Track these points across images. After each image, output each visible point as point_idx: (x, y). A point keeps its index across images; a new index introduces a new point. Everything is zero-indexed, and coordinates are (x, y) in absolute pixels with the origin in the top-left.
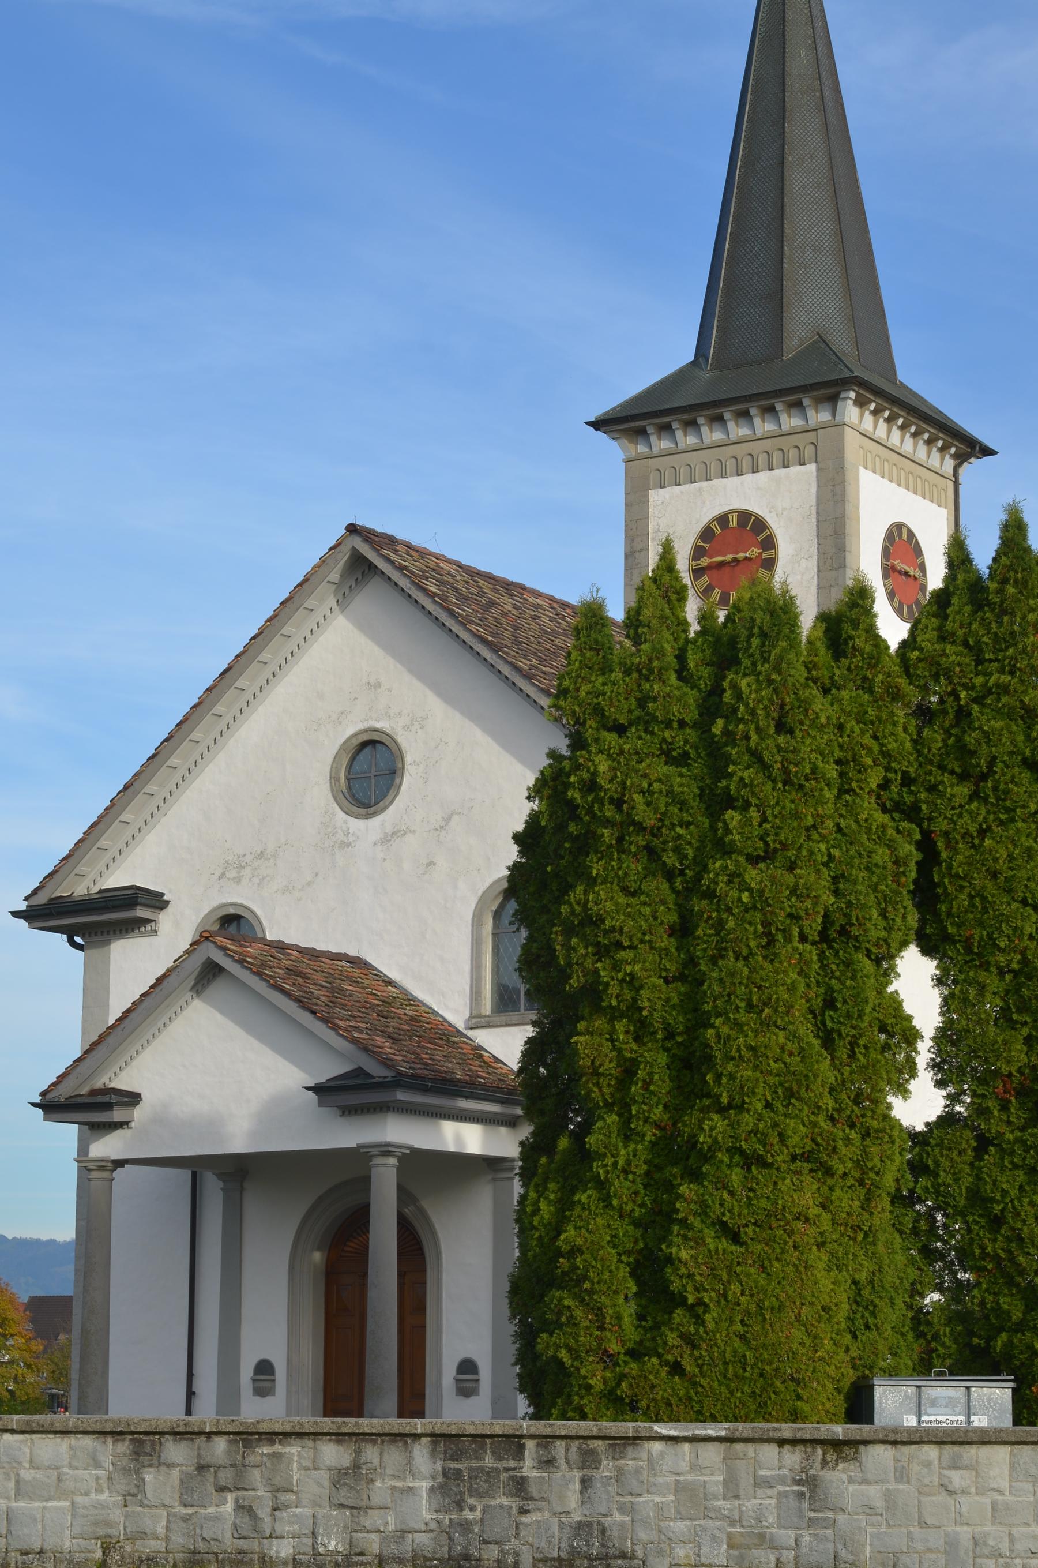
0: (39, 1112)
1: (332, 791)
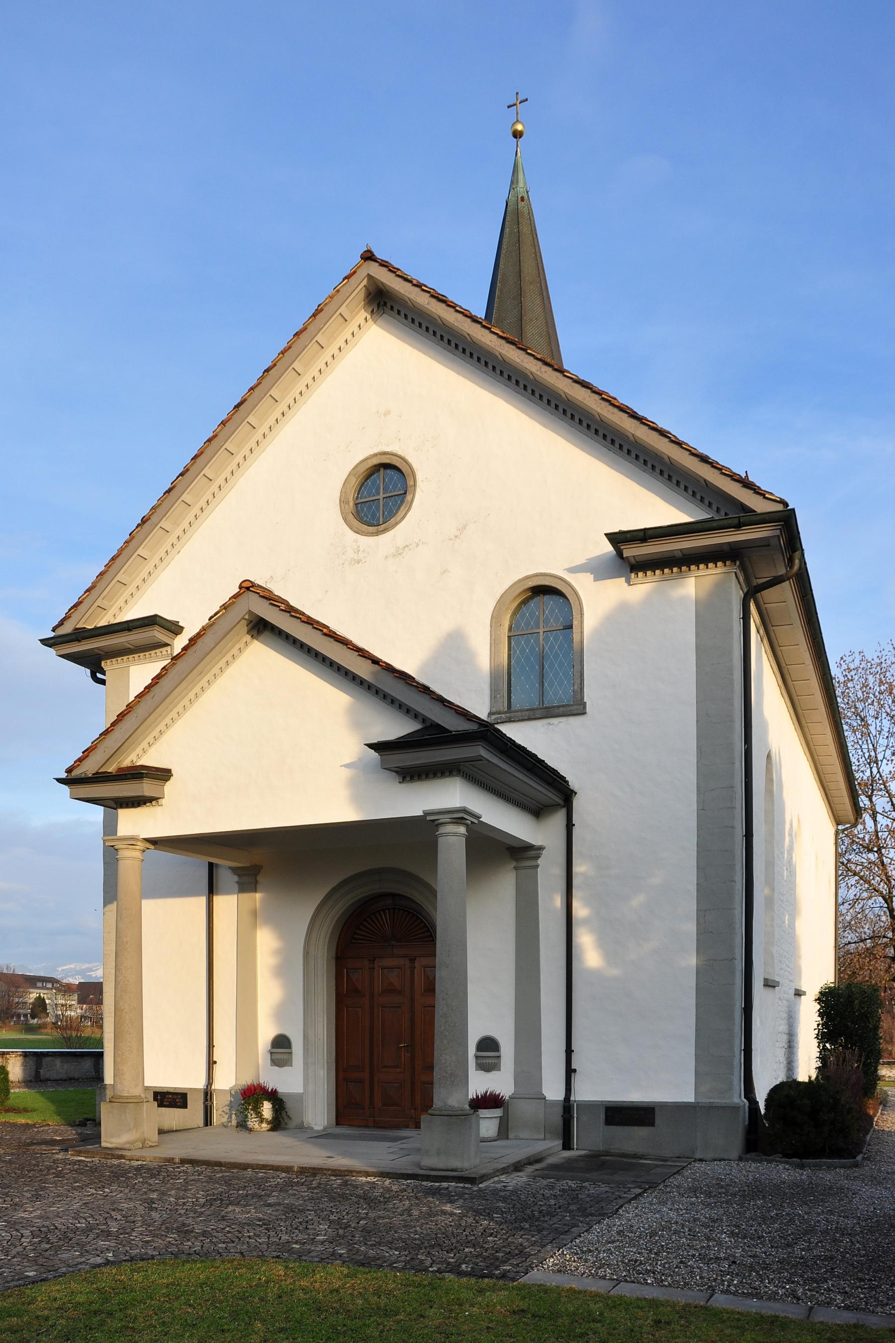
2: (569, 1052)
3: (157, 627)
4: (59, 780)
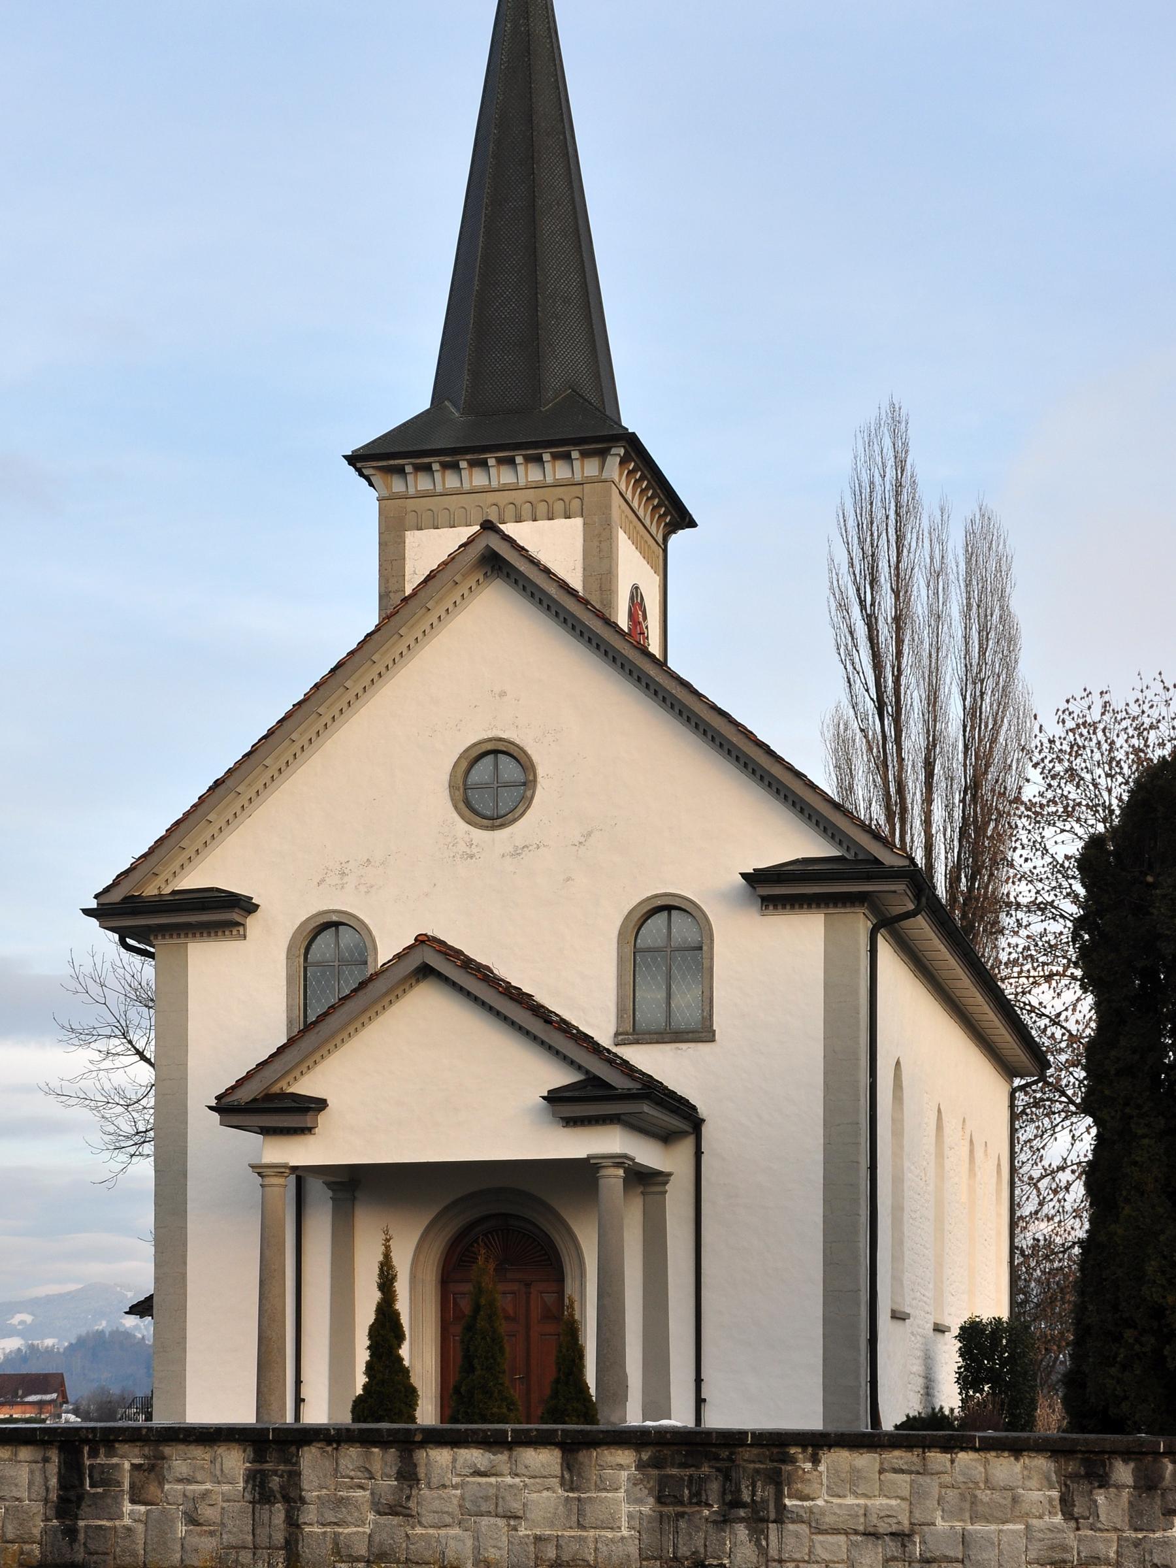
0: (216, 1116)
1: (452, 800)
2: (699, 1381)
3: (237, 910)
4: (210, 1108)
